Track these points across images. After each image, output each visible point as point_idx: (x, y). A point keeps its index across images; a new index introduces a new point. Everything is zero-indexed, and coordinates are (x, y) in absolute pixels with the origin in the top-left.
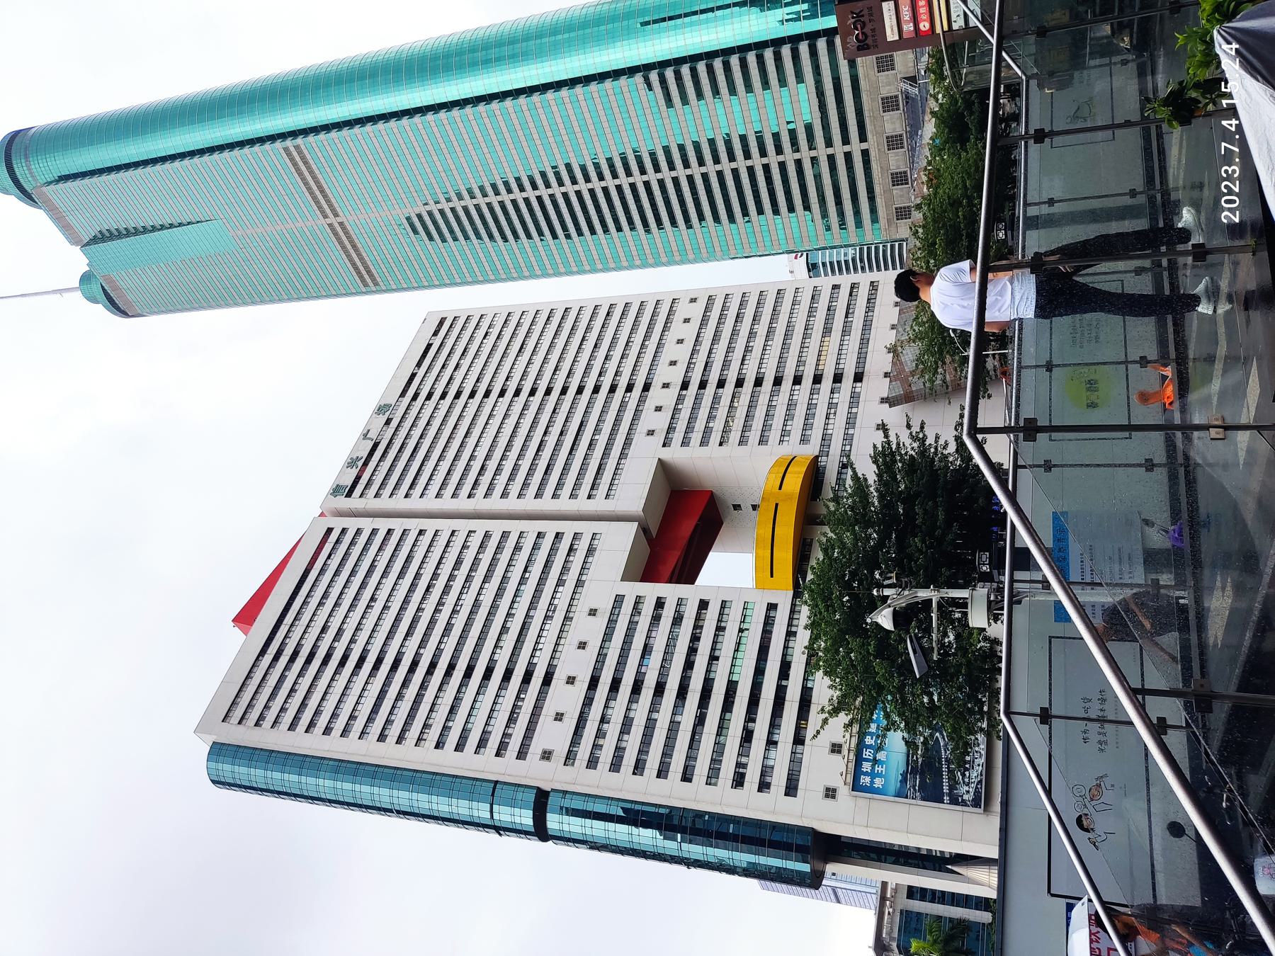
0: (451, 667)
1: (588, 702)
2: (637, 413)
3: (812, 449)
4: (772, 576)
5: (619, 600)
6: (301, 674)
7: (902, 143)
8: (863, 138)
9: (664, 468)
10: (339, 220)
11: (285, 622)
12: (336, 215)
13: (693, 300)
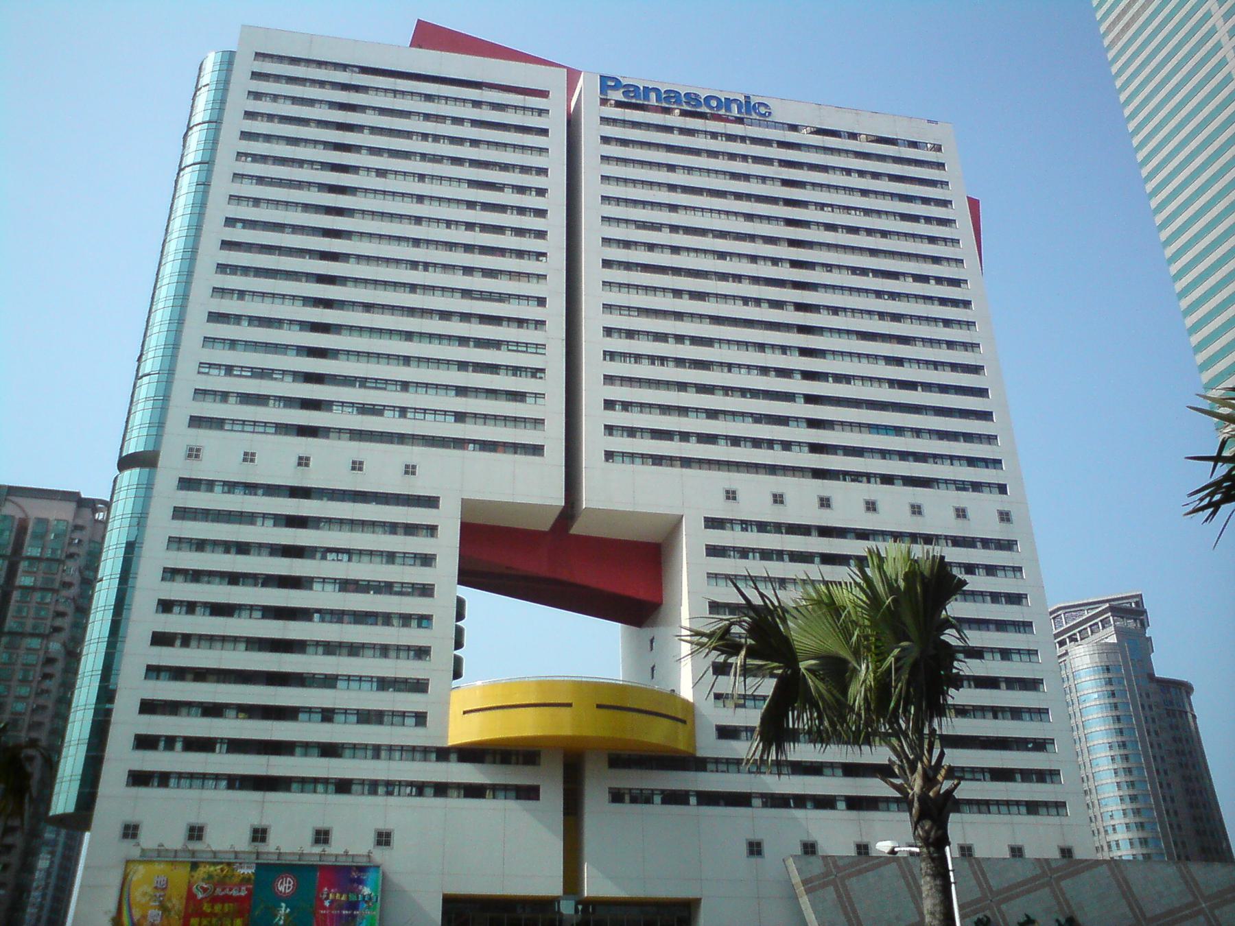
0: (328, 304)
1: (272, 490)
3: (709, 746)
4: (465, 713)
5: (431, 502)
11: (399, 81)
13: (1005, 517)
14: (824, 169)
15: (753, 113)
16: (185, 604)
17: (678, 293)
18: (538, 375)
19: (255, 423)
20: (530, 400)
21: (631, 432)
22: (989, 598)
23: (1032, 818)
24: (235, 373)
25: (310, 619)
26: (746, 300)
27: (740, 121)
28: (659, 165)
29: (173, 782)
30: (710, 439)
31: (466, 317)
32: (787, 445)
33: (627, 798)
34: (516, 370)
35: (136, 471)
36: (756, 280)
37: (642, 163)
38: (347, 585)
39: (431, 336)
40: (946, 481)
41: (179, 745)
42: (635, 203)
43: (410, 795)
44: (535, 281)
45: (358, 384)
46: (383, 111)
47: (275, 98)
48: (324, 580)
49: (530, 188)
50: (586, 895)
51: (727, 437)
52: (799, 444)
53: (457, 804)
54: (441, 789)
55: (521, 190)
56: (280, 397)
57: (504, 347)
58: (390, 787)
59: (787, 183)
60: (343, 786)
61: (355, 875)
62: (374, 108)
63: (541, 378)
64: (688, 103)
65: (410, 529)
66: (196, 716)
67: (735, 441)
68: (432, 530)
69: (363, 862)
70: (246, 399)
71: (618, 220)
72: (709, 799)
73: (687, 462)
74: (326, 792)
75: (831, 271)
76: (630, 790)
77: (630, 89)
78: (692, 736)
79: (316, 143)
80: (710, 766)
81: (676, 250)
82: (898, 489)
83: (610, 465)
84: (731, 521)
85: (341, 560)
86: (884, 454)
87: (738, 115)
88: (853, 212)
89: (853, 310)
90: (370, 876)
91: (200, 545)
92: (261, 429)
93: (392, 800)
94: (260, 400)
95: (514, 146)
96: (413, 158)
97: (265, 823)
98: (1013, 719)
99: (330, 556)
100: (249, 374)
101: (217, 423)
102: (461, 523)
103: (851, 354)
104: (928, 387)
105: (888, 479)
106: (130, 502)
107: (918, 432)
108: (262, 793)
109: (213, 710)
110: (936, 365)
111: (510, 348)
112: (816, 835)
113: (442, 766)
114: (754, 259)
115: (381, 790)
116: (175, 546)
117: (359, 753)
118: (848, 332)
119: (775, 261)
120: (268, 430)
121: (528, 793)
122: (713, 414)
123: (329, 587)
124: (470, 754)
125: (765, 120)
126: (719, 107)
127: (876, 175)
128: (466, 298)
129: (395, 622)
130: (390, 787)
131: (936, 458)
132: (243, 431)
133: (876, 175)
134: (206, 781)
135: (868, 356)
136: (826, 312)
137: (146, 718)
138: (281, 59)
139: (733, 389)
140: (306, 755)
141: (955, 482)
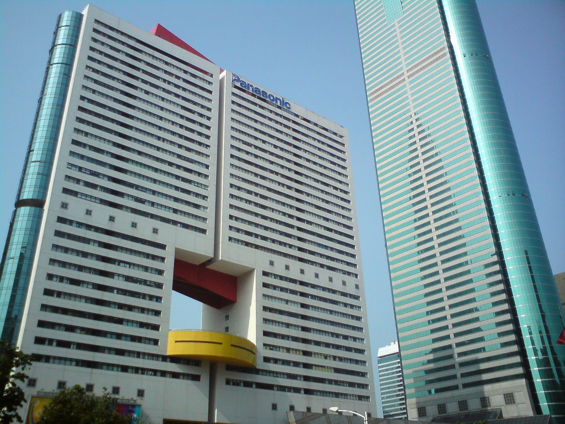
1: (97, 230)
2: (285, 255)
3: (261, 365)
4: (176, 342)
6: (123, 62)
7: (462, 410)
8: (465, 386)
9: (249, 273)
10: (406, 79)
11: (155, 52)
12: (409, 77)
13: (357, 287)
14: (307, 136)
15: (284, 106)
16: (59, 277)
17: (256, 175)
18: (205, 199)
19: (91, 197)
20: (202, 209)
21: (238, 230)
22: (351, 317)
23: (360, 402)
24: (83, 171)
25: (112, 292)
26: (279, 183)
27: (279, 108)
28: (252, 119)
29: (51, 360)
30: (264, 238)
31: (179, 167)
32: (291, 246)
33: (231, 383)
34: (197, 195)
35: (28, 208)
36: (283, 176)
37: (246, 116)
38: (128, 279)
39: (165, 172)
40: (340, 270)
41: (55, 343)
42: (243, 132)
43: (151, 375)
44: (205, 157)
45: (135, 188)
46: (148, 64)
47: (103, 44)
48: (119, 275)
49: (205, 116)
50: (216, 422)
51: (271, 239)
52: (295, 246)
53: (169, 380)
54: (163, 373)
55: (201, 115)
56: (102, 187)
57: (193, 184)
58: (143, 371)
59: (295, 138)
60: (125, 369)
61: (130, 408)
62: (145, 62)
63: (206, 200)
64: (263, 95)
65: (154, 257)
66: (63, 330)
67: (274, 241)
68: (163, 259)
69: (132, 402)
70: (87, 184)
71: (237, 139)
72: (261, 386)
73: (257, 247)
74: (117, 371)
75: (307, 178)
76: (233, 380)
77: (243, 83)
78: (254, 360)
79: (120, 70)
80: (260, 373)
81: (256, 156)
82: (325, 270)
83: (230, 243)
84: (271, 274)
85: (126, 267)
86: (321, 255)
87: (280, 106)
88: (315, 156)
89: (314, 196)
90: (137, 409)
91: (66, 250)
92: (94, 200)
93: (145, 377)
94: (94, 186)
95: (199, 95)
96: (159, 89)
97: (92, 383)
98: (356, 364)
99: (122, 264)
100: (89, 173)
101: (75, 193)
102: (175, 259)
103: (313, 214)
104: (336, 232)
105: (322, 266)
106: (25, 223)
107: (332, 249)
108: (91, 369)
109: (70, 329)
110: (339, 224)
111: (195, 184)
112: (294, 403)
113: (164, 363)
114: (282, 167)
115: (140, 371)
116: (55, 249)
117: (132, 354)
118: (312, 204)
119: (290, 170)
120: (97, 201)
121: (196, 378)
122: (266, 228)
123: (121, 278)
124: (175, 359)
125: (288, 110)
126: (273, 100)
127: (323, 143)
128: (179, 158)
129: (147, 298)
130: (143, 371)
131: (337, 260)
132: (86, 199)
133: (323, 143)
134: (66, 361)
135: (318, 215)
136: (305, 194)
137: (40, 329)
138: (106, 26)
139: (274, 219)
140: (110, 353)
141: (342, 271)
